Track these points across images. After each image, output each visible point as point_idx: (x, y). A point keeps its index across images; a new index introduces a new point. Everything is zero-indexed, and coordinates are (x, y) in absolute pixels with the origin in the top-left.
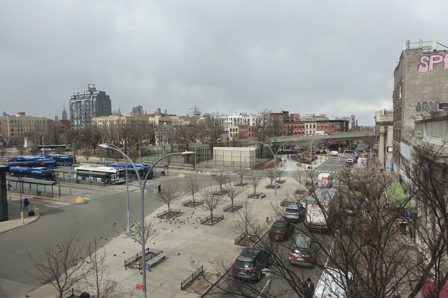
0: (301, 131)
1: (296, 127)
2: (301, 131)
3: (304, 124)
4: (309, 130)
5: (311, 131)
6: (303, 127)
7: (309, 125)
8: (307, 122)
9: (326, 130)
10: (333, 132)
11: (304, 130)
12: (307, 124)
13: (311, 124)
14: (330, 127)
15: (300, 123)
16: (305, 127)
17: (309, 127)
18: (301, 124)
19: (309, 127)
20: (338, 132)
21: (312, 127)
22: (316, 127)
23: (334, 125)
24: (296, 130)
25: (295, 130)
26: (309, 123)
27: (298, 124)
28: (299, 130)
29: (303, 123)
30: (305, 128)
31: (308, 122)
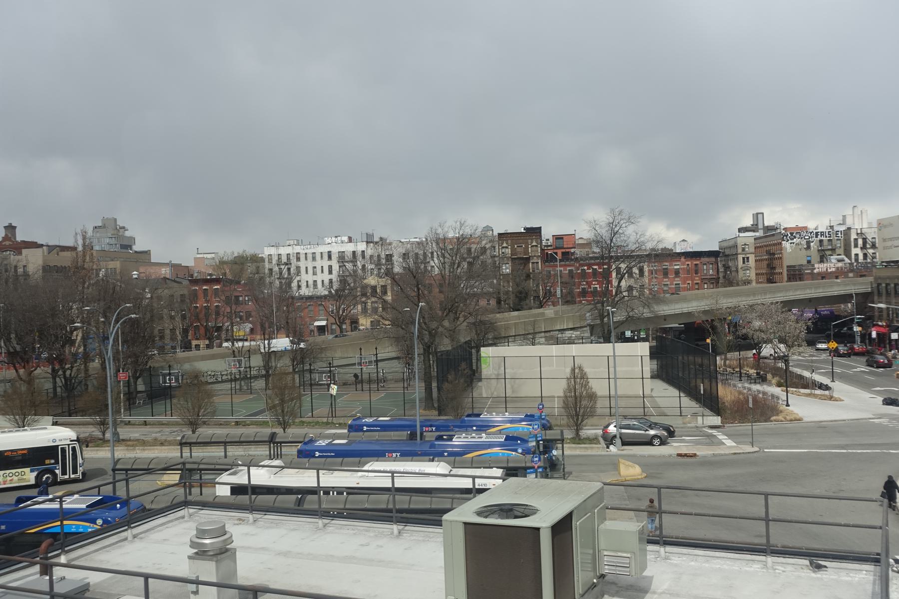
1: (584, 275)
9: (678, 281)
10: (697, 287)
14: (688, 272)
20: (712, 286)
22: (646, 274)
23: (699, 266)
25: (580, 284)
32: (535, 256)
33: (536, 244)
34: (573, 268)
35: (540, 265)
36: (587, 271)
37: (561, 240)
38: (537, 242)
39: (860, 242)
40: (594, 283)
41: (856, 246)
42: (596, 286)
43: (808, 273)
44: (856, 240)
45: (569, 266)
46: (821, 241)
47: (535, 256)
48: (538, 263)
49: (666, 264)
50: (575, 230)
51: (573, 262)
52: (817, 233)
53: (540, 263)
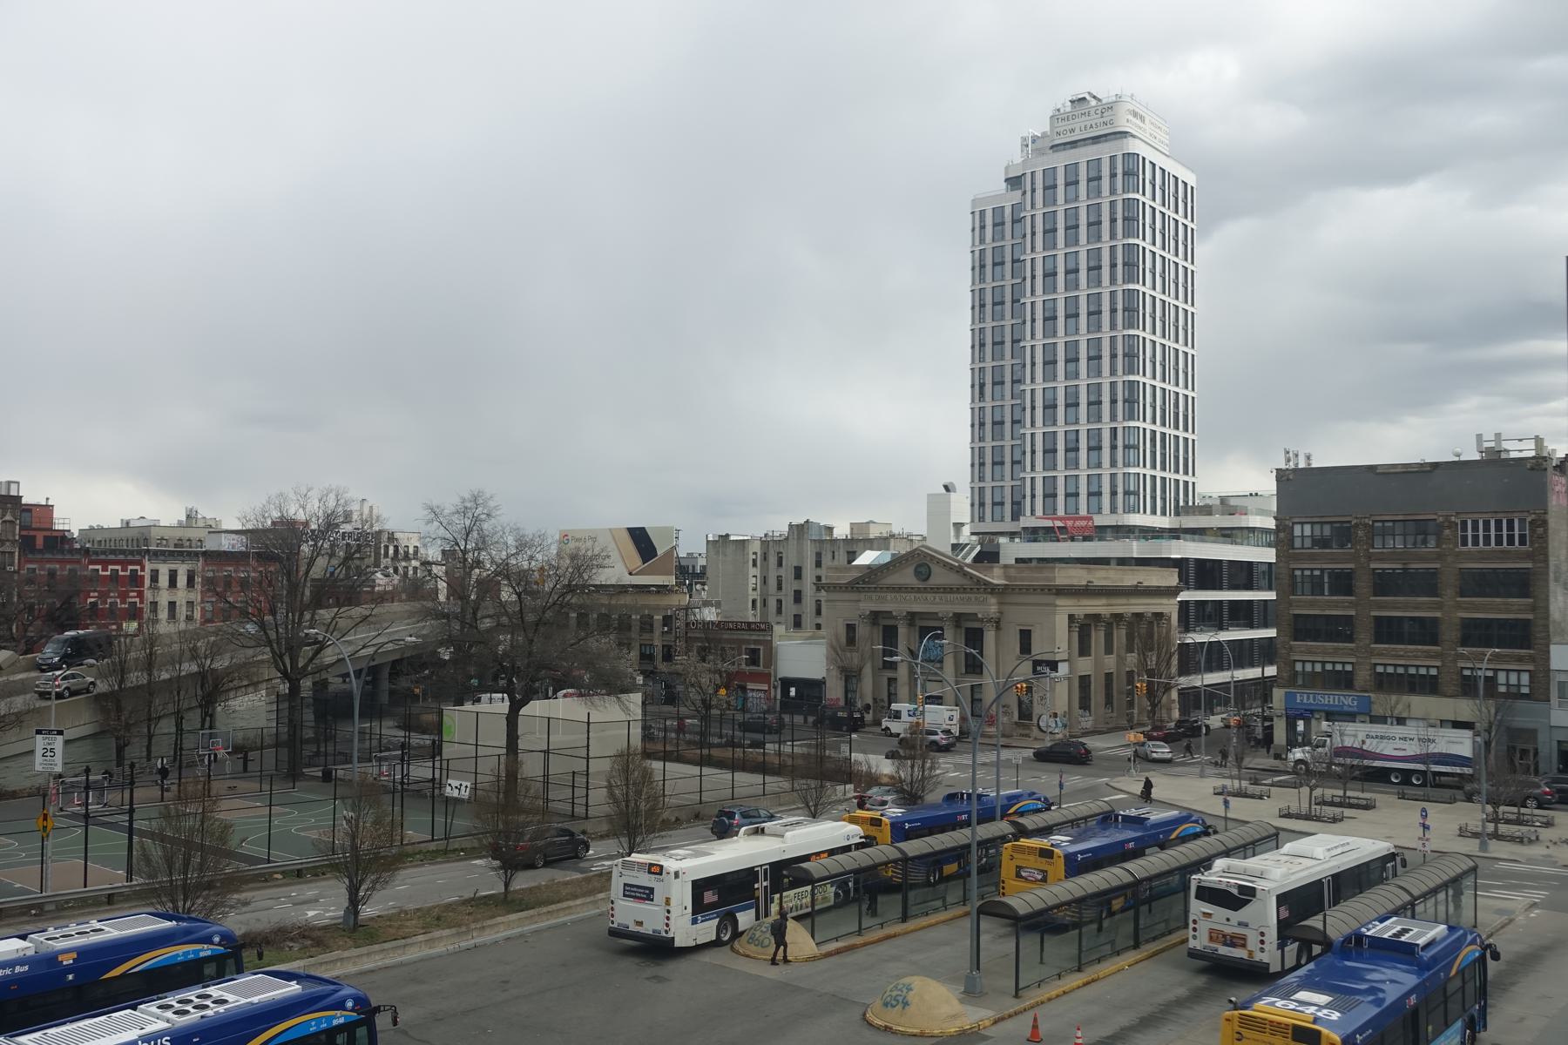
0: (123, 602)
2: (123, 602)
3: (140, 563)
4: (164, 598)
5: (172, 605)
6: (136, 580)
7: (164, 570)
8: (156, 555)
11: (140, 595)
12: (155, 566)
13: (173, 567)
15: (121, 557)
16: (147, 582)
17: (164, 580)
18: (124, 564)
19: (164, 580)
21: (182, 580)
24: (113, 598)
26: (164, 562)
27: (105, 564)
28: (113, 598)
29: (138, 557)
30: (142, 585)
31: (163, 553)
32: (8, 540)
33: (12, 519)
34: (77, 566)
35: (17, 557)
36: (101, 573)
37: (28, 514)
38: (14, 516)
39: (391, 551)
40: (112, 594)
41: (386, 555)
42: (133, 600)
43: (368, 592)
44: (387, 547)
45: (49, 561)
46: (348, 544)
47: (8, 540)
48: (14, 553)
49: (230, 568)
50: (47, 499)
51: (77, 557)
52: (344, 533)
53: (17, 554)
